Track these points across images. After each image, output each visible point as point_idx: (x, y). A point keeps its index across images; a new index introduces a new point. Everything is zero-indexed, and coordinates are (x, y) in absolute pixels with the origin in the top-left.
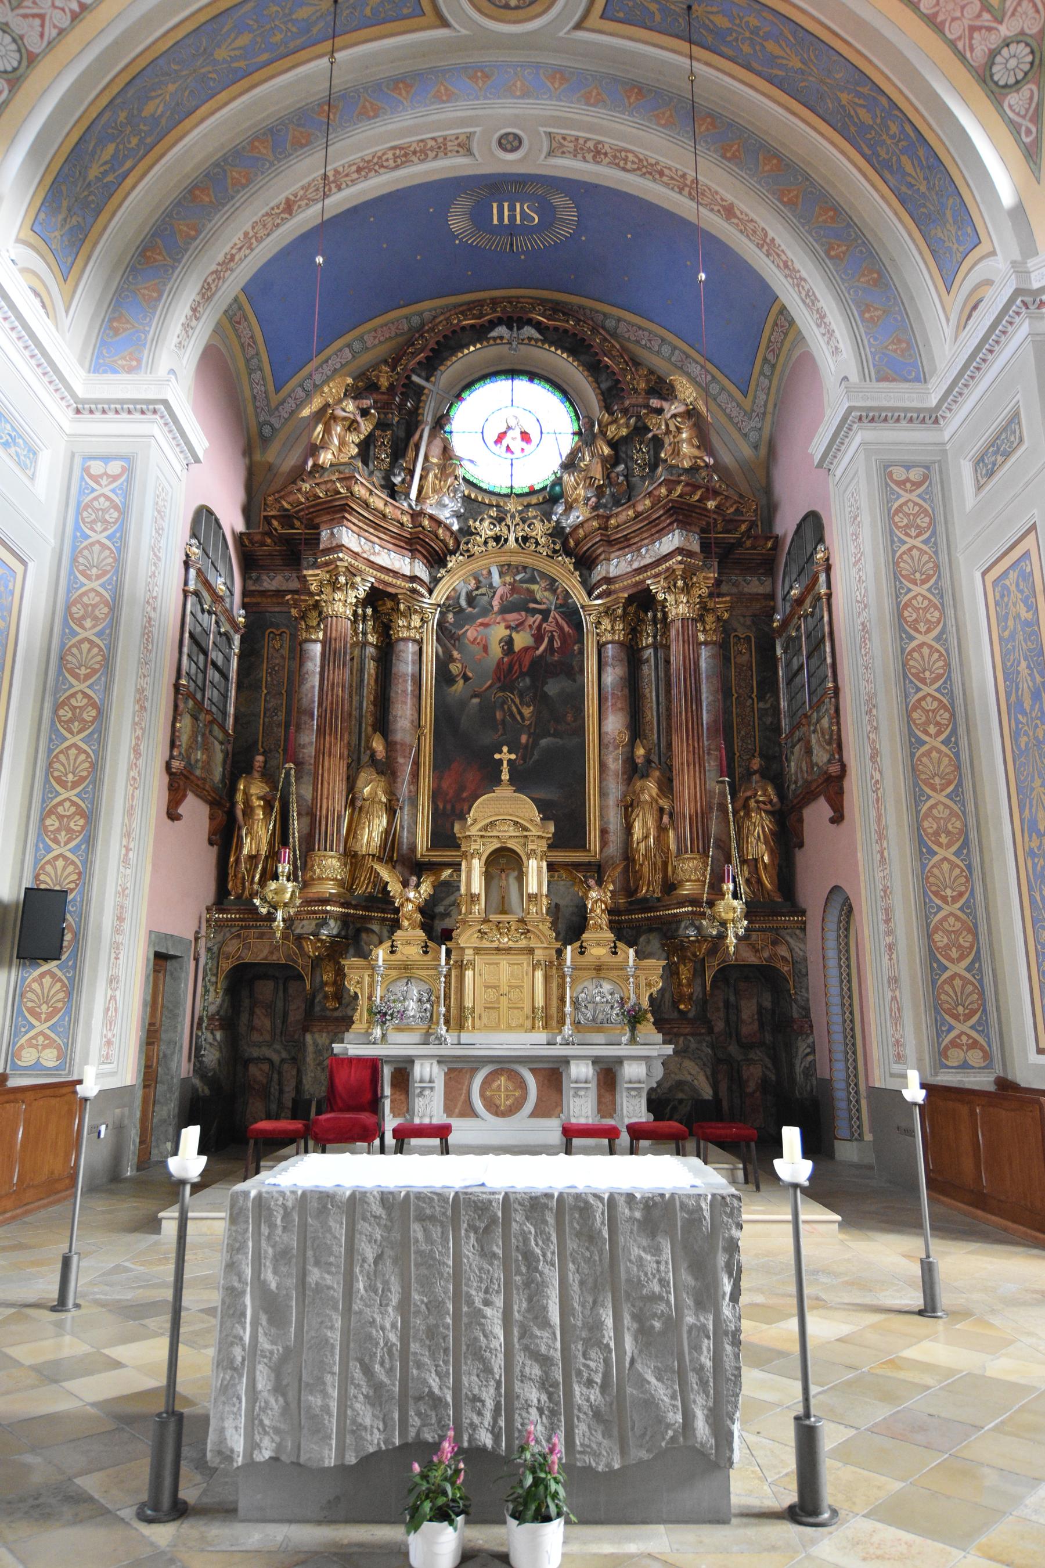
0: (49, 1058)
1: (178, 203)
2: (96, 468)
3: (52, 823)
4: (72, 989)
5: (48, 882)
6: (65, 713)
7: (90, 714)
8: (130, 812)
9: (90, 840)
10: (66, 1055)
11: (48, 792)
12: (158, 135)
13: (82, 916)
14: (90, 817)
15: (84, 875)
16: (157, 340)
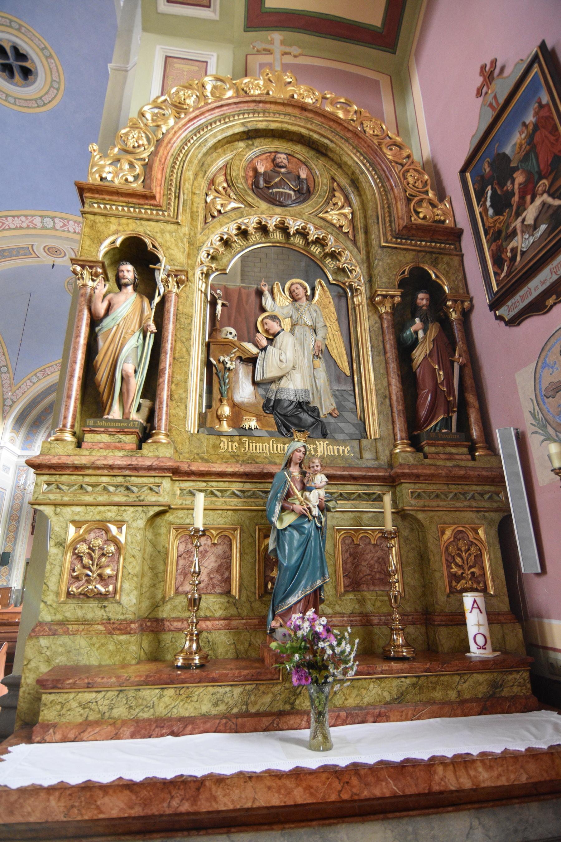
0: (5, 583)
1: (42, 412)
2: (22, 468)
3: (8, 539)
4: (10, 571)
5: (7, 551)
6: (12, 518)
7: (17, 518)
8: (23, 536)
9: (15, 543)
10: (8, 583)
11: (8, 533)
12: (39, 402)
13: (13, 557)
14: (16, 538)
15: (14, 549)
16: (36, 442)
